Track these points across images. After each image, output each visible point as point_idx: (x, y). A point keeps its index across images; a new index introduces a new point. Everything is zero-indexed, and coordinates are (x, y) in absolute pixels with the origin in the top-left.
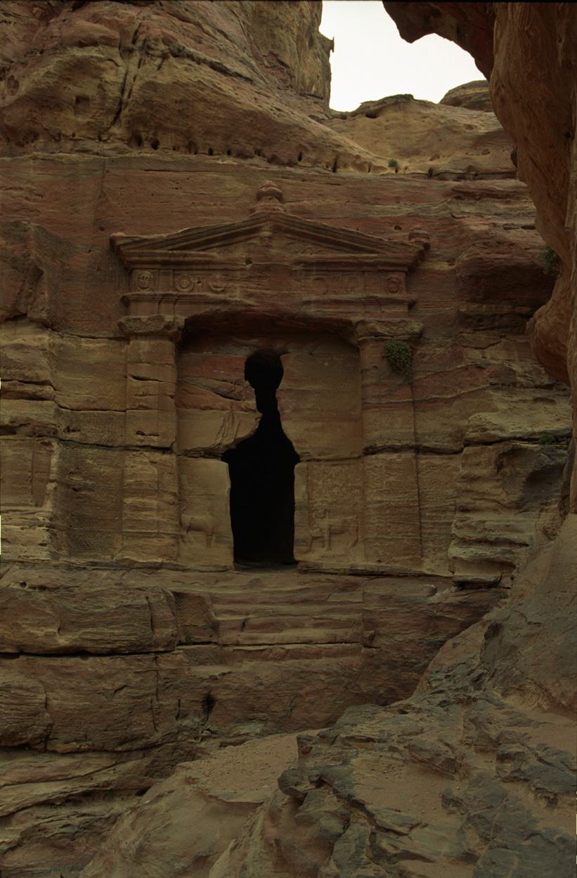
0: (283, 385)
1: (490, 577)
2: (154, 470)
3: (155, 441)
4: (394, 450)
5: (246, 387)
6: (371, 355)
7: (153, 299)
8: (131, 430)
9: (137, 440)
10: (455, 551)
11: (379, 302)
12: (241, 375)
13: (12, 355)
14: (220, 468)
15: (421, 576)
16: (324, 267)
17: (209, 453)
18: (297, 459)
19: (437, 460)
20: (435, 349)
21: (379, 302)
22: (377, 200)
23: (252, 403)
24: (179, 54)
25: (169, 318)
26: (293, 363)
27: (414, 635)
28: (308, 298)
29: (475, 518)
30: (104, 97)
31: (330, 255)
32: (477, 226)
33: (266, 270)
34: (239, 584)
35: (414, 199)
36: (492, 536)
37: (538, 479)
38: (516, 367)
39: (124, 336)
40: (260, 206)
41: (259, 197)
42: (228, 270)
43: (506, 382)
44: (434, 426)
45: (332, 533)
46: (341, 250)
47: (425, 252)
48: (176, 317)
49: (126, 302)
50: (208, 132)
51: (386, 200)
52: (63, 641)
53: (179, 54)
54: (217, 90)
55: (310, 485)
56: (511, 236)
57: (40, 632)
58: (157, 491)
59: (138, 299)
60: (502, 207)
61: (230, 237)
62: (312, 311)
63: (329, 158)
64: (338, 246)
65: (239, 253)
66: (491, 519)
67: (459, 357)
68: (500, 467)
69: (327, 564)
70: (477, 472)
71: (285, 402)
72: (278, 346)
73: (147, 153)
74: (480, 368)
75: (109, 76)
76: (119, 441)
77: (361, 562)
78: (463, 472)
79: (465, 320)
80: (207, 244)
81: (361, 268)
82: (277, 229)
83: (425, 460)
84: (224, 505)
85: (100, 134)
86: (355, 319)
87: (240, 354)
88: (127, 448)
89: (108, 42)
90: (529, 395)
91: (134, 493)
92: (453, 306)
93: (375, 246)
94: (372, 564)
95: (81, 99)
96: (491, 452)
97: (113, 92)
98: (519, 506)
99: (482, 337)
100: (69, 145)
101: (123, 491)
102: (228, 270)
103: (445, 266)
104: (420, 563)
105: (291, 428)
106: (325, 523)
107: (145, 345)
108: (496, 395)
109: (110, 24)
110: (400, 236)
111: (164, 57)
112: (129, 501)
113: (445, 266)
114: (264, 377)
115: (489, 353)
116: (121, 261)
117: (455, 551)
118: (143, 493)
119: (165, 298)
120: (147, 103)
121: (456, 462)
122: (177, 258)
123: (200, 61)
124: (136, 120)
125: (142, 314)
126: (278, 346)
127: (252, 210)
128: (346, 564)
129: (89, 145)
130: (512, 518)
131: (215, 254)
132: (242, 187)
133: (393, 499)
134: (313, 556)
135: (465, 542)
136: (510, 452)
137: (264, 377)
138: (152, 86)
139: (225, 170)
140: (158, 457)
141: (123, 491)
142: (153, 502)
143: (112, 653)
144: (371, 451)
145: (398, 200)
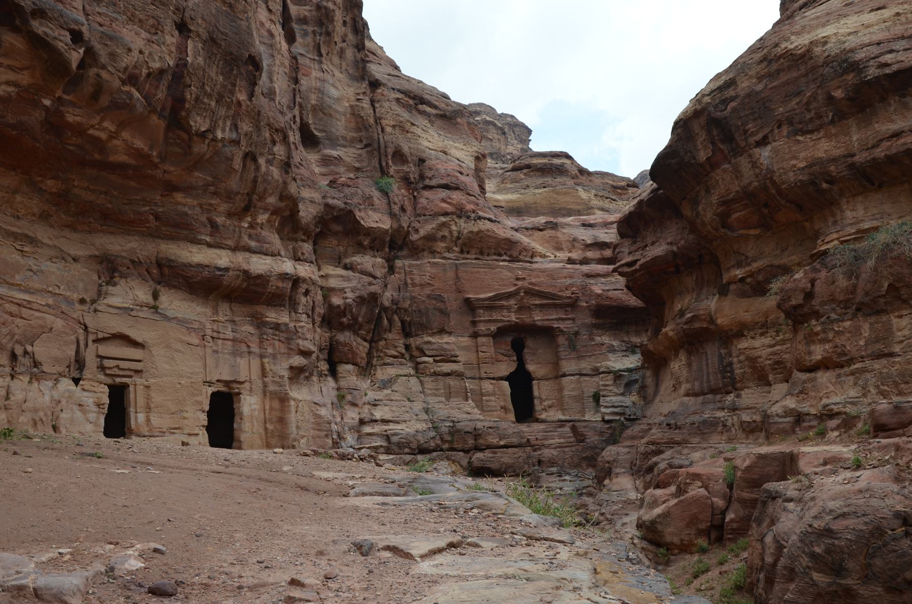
0: (526, 351)
1: (617, 418)
2: (491, 386)
3: (492, 376)
4: (572, 375)
5: (511, 352)
6: (561, 340)
7: (485, 321)
8: (482, 371)
9: (484, 375)
10: (603, 410)
11: (563, 319)
12: (509, 347)
13: (446, 346)
14: (506, 384)
15: (585, 421)
16: (542, 306)
17: (501, 379)
18: (533, 379)
19: (587, 378)
20: (584, 336)
21: (563, 319)
22: (558, 278)
23: (515, 358)
24: (480, 218)
25: (492, 329)
26: (530, 343)
27: (597, 438)
28: (538, 317)
29: (608, 399)
30: (452, 236)
31: (545, 302)
32: (597, 290)
33: (521, 309)
34: (523, 427)
35: (571, 277)
36: (616, 404)
37: (629, 385)
38: (614, 344)
39: (475, 335)
40: (520, 283)
41: (518, 279)
42: (508, 308)
43: (612, 350)
44: (585, 365)
45: (550, 407)
46: (551, 301)
47: (577, 299)
48: (493, 328)
49: (474, 323)
50: (489, 248)
51: (561, 278)
52: (502, 443)
53: (480, 218)
54: (494, 232)
55: (539, 389)
56: (610, 294)
57: (495, 441)
58: (494, 394)
59: (480, 321)
60: (603, 280)
61: (509, 296)
62: (539, 323)
63: (531, 253)
64: (547, 298)
65: (512, 302)
66: (614, 399)
67: (593, 340)
68: (615, 381)
69: (549, 419)
70: (607, 383)
71: (528, 357)
72: (523, 335)
73: (466, 256)
74: (602, 345)
75: (454, 228)
76: (478, 376)
77: (563, 418)
78: (601, 383)
79: (595, 326)
80: (501, 299)
81: (555, 306)
82: (525, 292)
83: (583, 378)
84: (509, 399)
85: (449, 250)
86: (555, 326)
87: (509, 339)
88: (481, 379)
89: (452, 213)
90: (620, 354)
91: (486, 396)
92: (589, 320)
93: (561, 297)
94: (568, 418)
95: (444, 237)
96: (611, 376)
97: (455, 234)
98: (622, 394)
99: (600, 331)
100: (438, 255)
101: (482, 395)
102: (508, 308)
103: (585, 304)
104: (584, 416)
105: (531, 367)
106: (546, 403)
107: (484, 339)
108: (610, 355)
109: (449, 203)
110: (568, 293)
111: (475, 220)
112: (484, 398)
113: (585, 304)
114: (518, 348)
115: (603, 337)
116: (470, 306)
117: (603, 410)
118: (489, 395)
119: (490, 321)
120: (469, 239)
121: (596, 379)
122: (492, 304)
123: (485, 218)
124: (465, 244)
125: (482, 327)
126: (523, 335)
127: (516, 285)
128: (556, 418)
129: (447, 255)
130: (621, 398)
131: (504, 303)
132: (510, 274)
133: (574, 393)
134: (543, 416)
135: (606, 407)
136: (618, 376)
137: (518, 348)
138: (471, 232)
139: (502, 267)
140: (492, 381)
141: (482, 395)
142: (493, 398)
143: (515, 447)
144: (564, 375)
145: (565, 277)
